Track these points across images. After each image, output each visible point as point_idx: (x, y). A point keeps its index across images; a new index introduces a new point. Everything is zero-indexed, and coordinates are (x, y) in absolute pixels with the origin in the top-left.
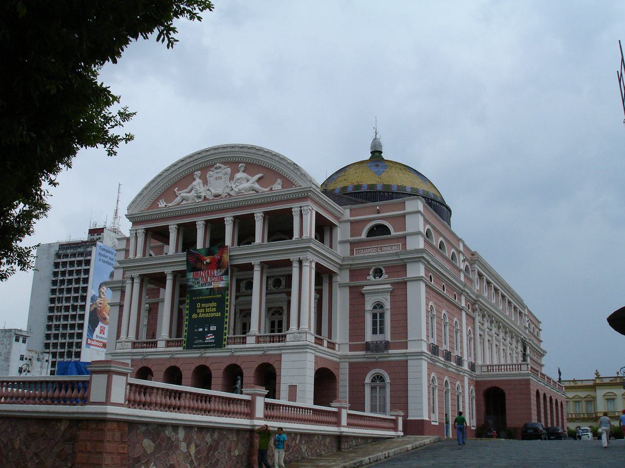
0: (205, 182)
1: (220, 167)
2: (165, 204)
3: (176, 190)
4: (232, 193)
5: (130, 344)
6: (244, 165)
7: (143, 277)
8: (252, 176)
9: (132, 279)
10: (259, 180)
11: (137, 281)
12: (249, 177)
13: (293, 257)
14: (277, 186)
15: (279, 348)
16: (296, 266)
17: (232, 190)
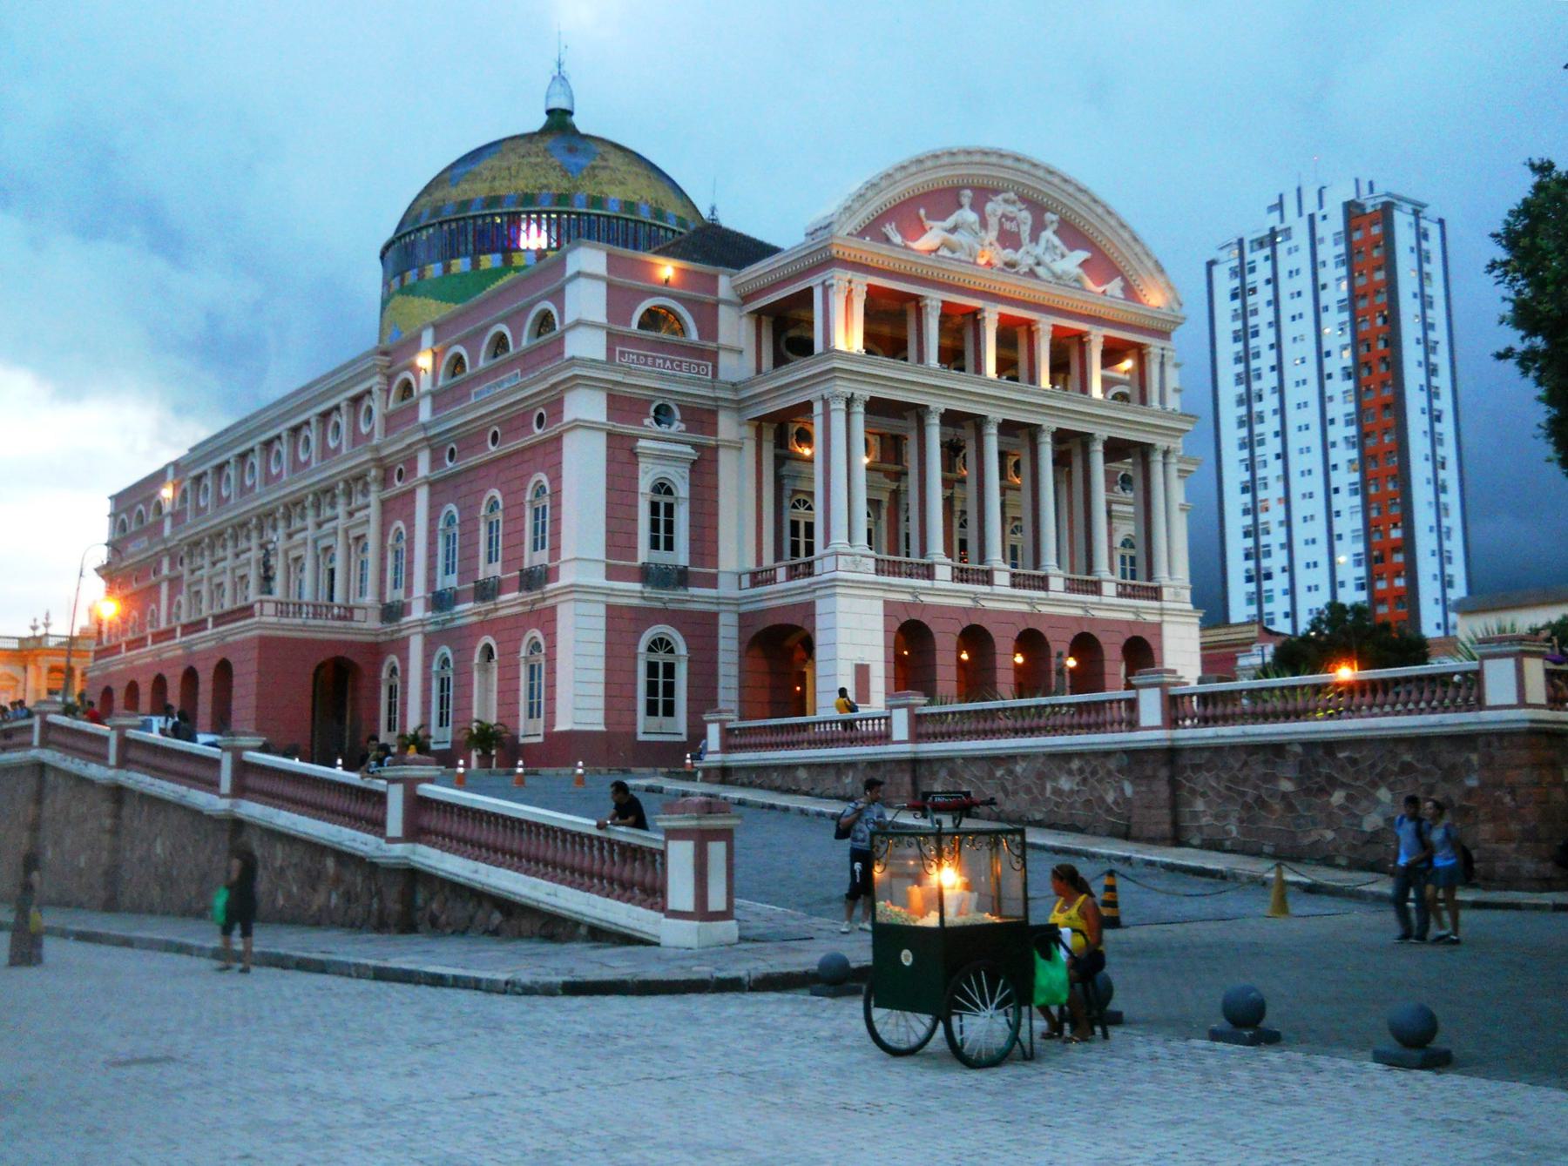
0: (984, 224)
1: (1014, 203)
2: (897, 239)
3: (922, 212)
4: (1040, 271)
5: (871, 564)
6: (1054, 218)
7: (876, 407)
8: (1072, 248)
9: (849, 402)
10: (1084, 264)
11: (859, 409)
12: (1066, 251)
13: (1161, 442)
14: (1115, 288)
15: (1162, 611)
16: (1157, 458)
17: (1038, 264)
